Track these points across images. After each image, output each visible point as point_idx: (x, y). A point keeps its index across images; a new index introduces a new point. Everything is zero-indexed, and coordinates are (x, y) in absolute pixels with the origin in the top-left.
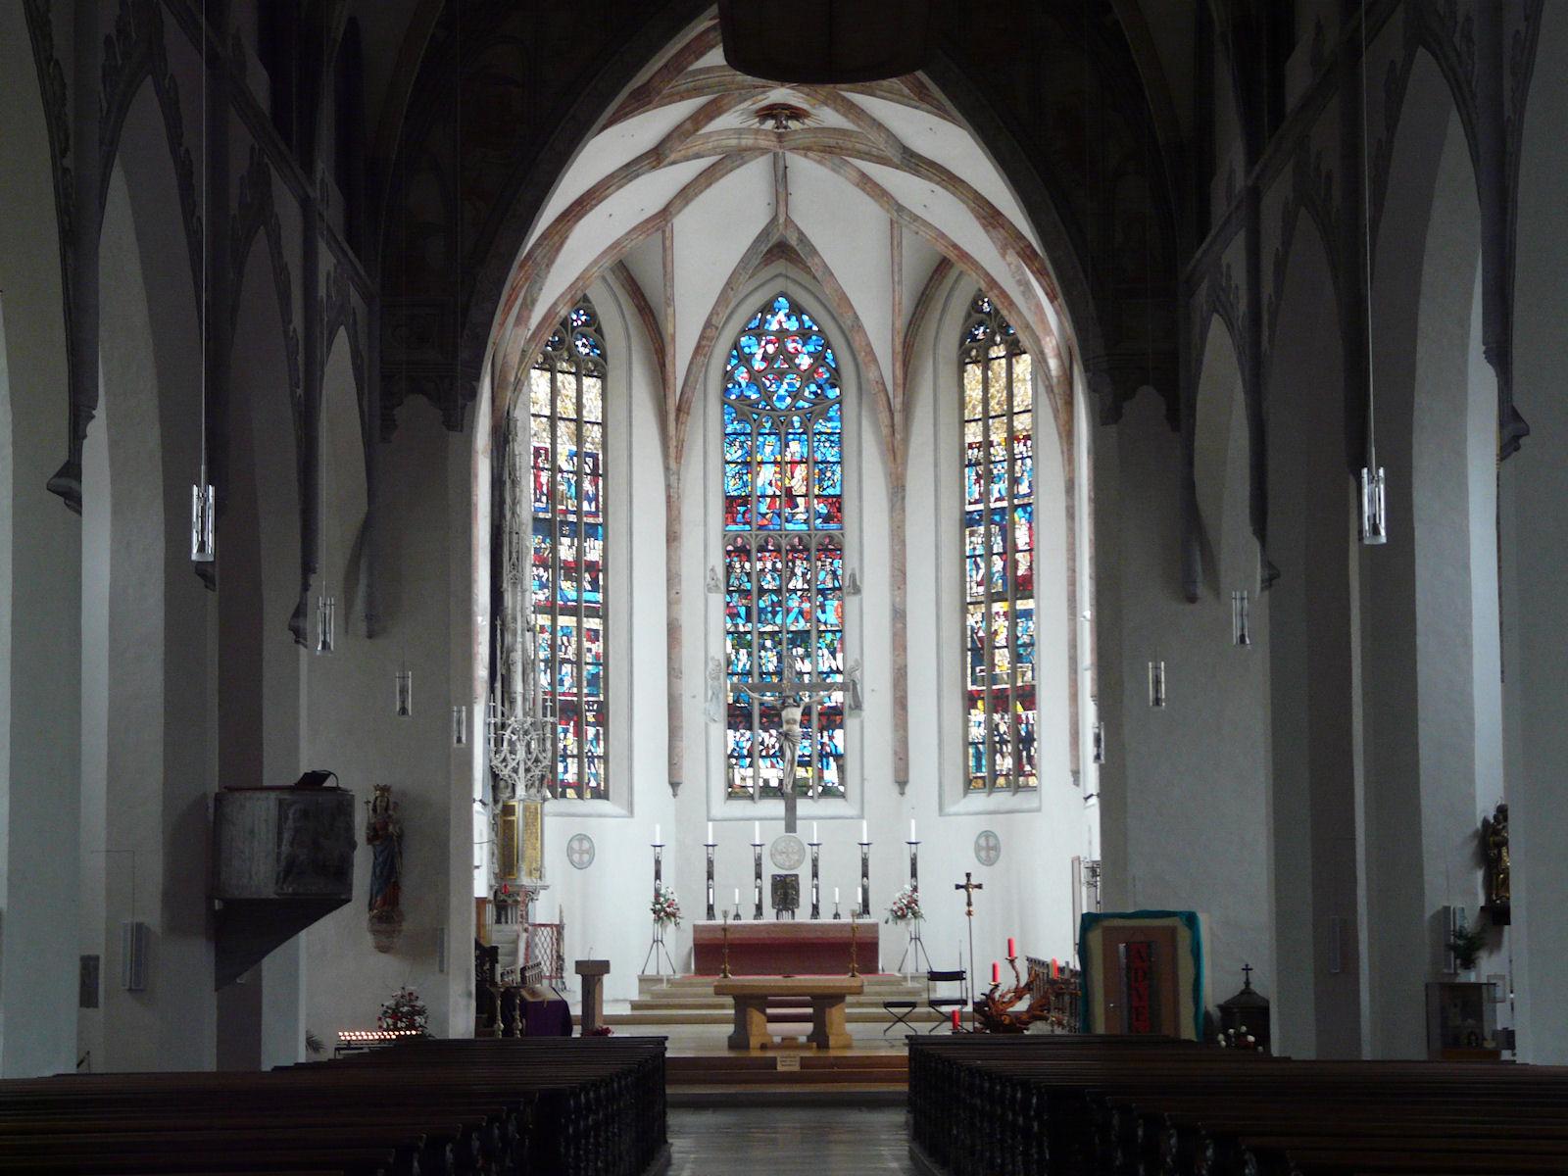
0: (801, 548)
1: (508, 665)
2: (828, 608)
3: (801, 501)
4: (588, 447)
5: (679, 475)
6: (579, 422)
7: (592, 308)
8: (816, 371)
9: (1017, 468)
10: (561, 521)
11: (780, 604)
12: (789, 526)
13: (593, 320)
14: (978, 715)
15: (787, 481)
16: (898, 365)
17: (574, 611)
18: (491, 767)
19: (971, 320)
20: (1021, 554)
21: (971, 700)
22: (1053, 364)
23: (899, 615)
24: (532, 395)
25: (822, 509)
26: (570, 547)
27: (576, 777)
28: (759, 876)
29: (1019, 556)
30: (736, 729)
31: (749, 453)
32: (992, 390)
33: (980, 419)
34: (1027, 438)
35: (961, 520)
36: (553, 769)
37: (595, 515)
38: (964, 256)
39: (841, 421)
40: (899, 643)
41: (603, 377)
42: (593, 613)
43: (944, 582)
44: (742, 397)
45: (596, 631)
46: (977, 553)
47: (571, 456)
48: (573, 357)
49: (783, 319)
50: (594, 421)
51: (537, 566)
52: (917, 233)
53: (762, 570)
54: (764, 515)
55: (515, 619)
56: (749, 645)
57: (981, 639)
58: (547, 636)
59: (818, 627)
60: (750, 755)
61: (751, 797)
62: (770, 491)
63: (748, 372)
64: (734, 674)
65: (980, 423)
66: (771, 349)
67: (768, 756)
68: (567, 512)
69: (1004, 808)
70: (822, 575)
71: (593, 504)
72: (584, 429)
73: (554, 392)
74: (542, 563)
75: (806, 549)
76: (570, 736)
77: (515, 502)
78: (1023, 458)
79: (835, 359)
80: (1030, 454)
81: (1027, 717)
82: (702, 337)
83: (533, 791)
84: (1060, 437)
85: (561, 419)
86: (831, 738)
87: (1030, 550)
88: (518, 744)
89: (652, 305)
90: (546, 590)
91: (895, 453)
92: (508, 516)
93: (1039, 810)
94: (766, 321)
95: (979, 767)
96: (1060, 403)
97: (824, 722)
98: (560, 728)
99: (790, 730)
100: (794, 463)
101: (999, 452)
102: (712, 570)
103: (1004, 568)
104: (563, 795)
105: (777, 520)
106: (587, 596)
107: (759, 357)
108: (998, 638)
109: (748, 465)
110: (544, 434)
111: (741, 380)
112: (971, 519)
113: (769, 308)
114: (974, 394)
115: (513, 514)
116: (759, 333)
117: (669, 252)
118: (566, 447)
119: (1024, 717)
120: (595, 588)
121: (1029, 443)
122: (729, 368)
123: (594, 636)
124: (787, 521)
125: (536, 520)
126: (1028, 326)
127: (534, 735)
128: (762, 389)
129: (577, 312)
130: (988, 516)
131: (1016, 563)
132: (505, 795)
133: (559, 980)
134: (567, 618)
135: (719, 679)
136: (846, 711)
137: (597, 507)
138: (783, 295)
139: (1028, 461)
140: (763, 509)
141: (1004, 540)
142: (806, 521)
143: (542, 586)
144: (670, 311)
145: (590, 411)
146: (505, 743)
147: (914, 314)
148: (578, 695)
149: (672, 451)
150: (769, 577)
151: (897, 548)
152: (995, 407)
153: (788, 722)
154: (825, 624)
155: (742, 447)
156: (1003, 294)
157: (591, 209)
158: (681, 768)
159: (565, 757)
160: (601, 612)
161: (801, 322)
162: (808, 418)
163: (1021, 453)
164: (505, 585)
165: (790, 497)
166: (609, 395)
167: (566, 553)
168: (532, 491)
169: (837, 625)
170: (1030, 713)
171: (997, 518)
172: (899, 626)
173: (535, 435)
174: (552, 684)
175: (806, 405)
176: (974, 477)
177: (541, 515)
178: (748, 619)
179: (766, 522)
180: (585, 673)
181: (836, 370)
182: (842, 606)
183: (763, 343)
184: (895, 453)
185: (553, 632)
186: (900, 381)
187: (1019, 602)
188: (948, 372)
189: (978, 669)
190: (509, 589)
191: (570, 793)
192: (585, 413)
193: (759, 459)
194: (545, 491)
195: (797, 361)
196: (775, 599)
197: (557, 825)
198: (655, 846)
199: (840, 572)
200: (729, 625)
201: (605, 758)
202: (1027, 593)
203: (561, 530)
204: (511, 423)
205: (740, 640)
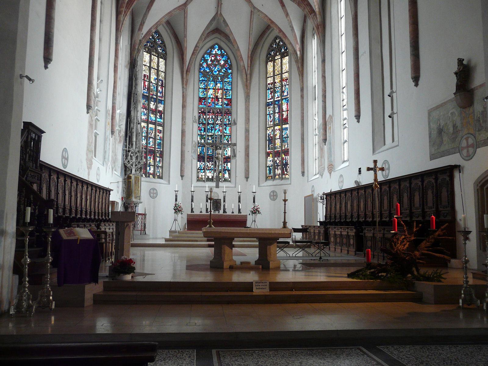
0: (220, 112)
1: (131, 133)
2: (227, 129)
3: (220, 100)
4: (160, 78)
5: (186, 89)
6: (158, 70)
7: (163, 39)
8: (225, 65)
9: (284, 88)
10: (151, 97)
11: (213, 127)
12: (217, 106)
13: (163, 42)
15: (216, 94)
16: (249, 62)
17: (154, 123)
19: (270, 50)
20: (284, 112)
22: (298, 53)
23: (247, 131)
24: (144, 59)
25: (226, 102)
26: (154, 105)
27: (153, 172)
29: (284, 113)
30: (200, 162)
31: (206, 86)
32: (276, 68)
33: (272, 76)
34: (287, 79)
35: (266, 104)
37: (162, 97)
38: (272, 22)
39: (232, 78)
40: (247, 138)
41: (165, 59)
42: (160, 125)
44: (204, 70)
46: (271, 113)
47: (155, 79)
48: (157, 52)
49: (217, 51)
50: (162, 71)
51: (143, 109)
52: (259, 15)
53: (209, 118)
54: (210, 103)
55: (134, 120)
56: (205, 138)
57: (271, 137)
58: (145, 129)
59: (224, 134)
60: (204, 169)
61: (204, 181)
62: (211, 97)
63: (207, 64)
64: (200, 146)
65: (272, 77)
66: (213, 58)
67: (209, 170)
68: (153, 95)
70: (226, 120)
71: (161, 94)
72: (159, 73)
73: (151, 60)
74: (144, 107)
75: (221, 113)
77: (136, 84)
78: (285, 85)
79: (230, 62)
80: (287, 84)
81: (286, 158)
82: (194, 50)
83: (138, 172)
85: (152, 68)
86: (227, 165)
87: (287, 111)
88: (133, 157)
89: (180, 41)
90: (146, 116)
91: (247, 87)
92: (134, 88)
93: (290, 184)
94: (212, 51)
95: (270, 173)
96: (300, 65)
97: (225, 160)
98: (148, 157)
99: (218, 156)
100: (218, 89)
101: (278, 85)
102: (195, 117)
103: (279, 116)
104: (149, 177)
105: (213, 104)
106: (158, 120)
107: (209, 60)
109: (206, 89)
110: (147, 71)
111: (205, 66)
112: (269, 104)
113: (213, 47)
114: (270, 70)
115: (135, 88)
116: (210, 54)
118: (153, 77)
119: (285, 158)
120: (161, 118)
121: (287, 81)
122: (201, 63)
123: (160, 132)
124: (216, 105)
125: (143, 95)
126: (291, 43)
127: (138, 154)
128: (210, 69)
130: (274, 103)
131: (283, 115)
132: (128, 173)
133: (144, 231)
134: (152, 125)
135: (196, 147)
136: (231, 158)
137: (162, 95)
139: (287, 86)
140: (210, 101)
141: (279, 109)
142: (221, 105)
143: (145, 115)
145: (161, 68)
146: (129, 156)
147: (254, 48)
148: (155, 148)
149: (185, 83)
150: (211, 120)
153: (217, 154)
154: (226, 133)
155: (204, 84)
156: (284, 33)
158: (184, 171)
159: (150, 165)
160: (162, 125)
161: (222, 52)
163: (285, 84)
164: (131, 109)
165: (217, 98)
166: (167, 64)
167: (152, 106)
168: (143, 87)
169: (229, 134)
170: (287, 157)
171: (277, 103)
172: (247, 134)
173: (144, 71)
174: (147, 143)
175: (222, 74)
177: (145, 94)
178: (204, 131)
179: (210, 105)
180: (157, 142)
181: (231, 65)
182: (231, 129)
183: (211, 57)
184: (247, 87)
185: (147, 128)
186: (250, 66)
189: (270, 145)
190: (133, 110)
191: (151, 176)
192: (160, 68)
193: (209, 88)
194: (147, 87)
195: (220, 62)
196: (212, 126)
197: (145, 185)
198: (176, 191)
199: (230, 119)
200: (199, 133)
201: (162, 167)
202: (286, 123)
204: (136, 61)
205: (202, 137)
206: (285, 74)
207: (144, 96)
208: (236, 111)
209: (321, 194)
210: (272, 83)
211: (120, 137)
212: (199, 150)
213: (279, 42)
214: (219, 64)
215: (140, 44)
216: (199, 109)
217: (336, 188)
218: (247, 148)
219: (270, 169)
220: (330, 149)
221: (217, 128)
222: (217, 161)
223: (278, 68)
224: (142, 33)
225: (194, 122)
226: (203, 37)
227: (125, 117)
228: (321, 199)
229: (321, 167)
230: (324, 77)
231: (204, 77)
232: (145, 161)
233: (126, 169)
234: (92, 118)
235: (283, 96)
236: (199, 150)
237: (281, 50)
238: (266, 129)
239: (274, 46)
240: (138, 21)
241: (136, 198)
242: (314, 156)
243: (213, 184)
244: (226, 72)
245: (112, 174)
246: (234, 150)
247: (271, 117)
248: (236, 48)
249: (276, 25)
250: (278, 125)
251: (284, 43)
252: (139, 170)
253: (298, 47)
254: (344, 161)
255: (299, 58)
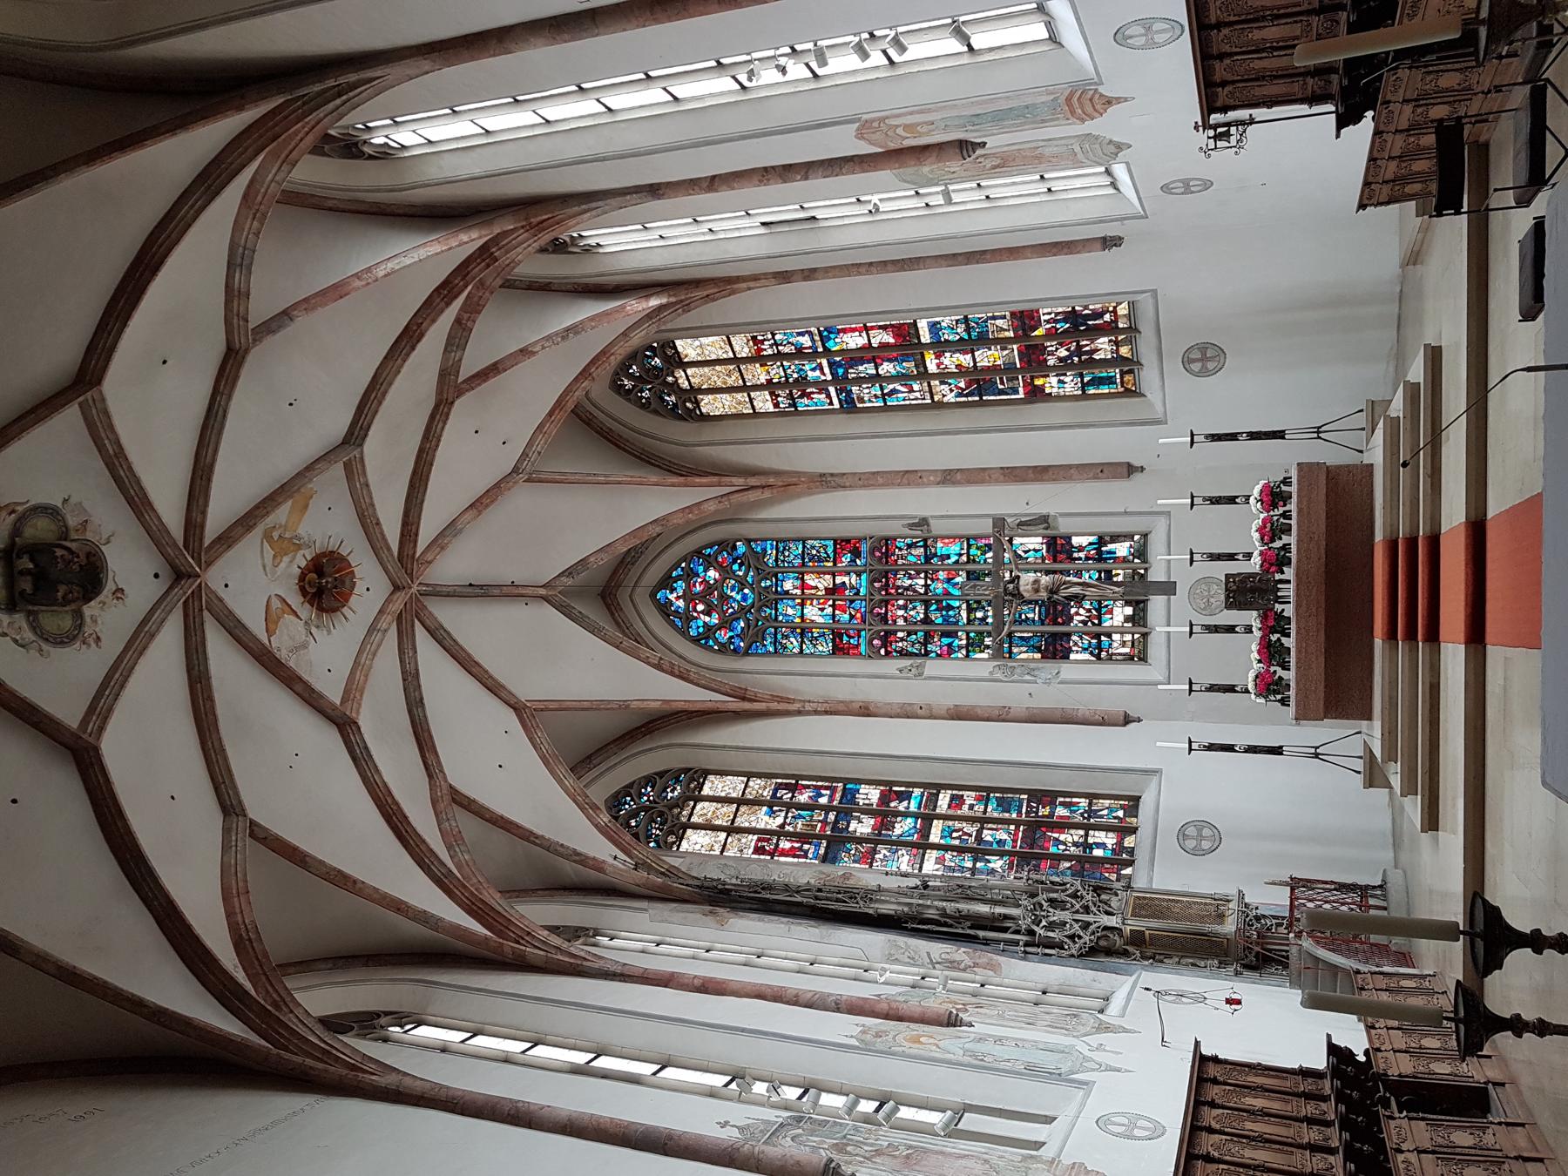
1: (960, 917)
2: (945, 551)
3: (839, 580)
4: (767, 794)
6: (741, 802)
9: (786, 350)
11: (939, 602)
12: (863, 591)
13: (649, 780)
14: (1051, 384)
16: (704, 480)
17: (927, 819)
18: (1081, 955)
21: (1036, 394)
22: (654, 302)
23: (949, 477)
27: (1111, 835)
28: (1231, 629)
30: (1070, 650)
31: (793, 630)
32: (719, 384)
34: (754, 338)
36: (1101, 861)
37: (833, 790)
38: (559, 404)
41: (706, 773)
43: (911, 428)
45: (953, 798)
47: (772, 813)
53: (906, 619)
54: (852, 617)
58: (948, 856)
60: (1097, 636)
61: (1145, 635)
62: (829, 610)
64: (1010, 652)
66: (700, 607)
67: (1099, 617)
68: (824, 822)
69: (1154, 340)
70: (911, 558)
73: (709, 827)
74: (869, 858)
76: (1062, 837)
77: (787, 888)
78: (776, 344)
81: (1048, 322)
82: (672, 674)
83: (1114, 903)
84: (733, 292)
86: (1081, 549)
87: (867, 329)
91: (789, 484)
92: (798, 899)
93: (1154, 292)
97: (1063, 556)
98: (1053, 850)
101: (776, 373)
103: (890, 360)
104: (1131, 851)
105: (857, 604)
107: (707, 619)
108: (965, 364)
109: (804, 630)
113: (665, 609)
116: (688, 618)
117: (564, 705)
118: (763, 819)
123: (956, 801)
125: (824, 859)
126: (624, 334)
127: (1042, 898)
129: (641, 795)
131: (883, 346)
137: (826, 788)
138: (653, 595)
140: (846, 617)
141: (862, 361)
142: (859, 575)
144: (634, 705)
146: (1051, 934)
148: (1017, 823)
149: (781, 708)
151: (881, 481)
152: (734, 380)
153: (1037, 591)
155: (787, 637)
157: (397, 804)
159: (1087, 846)
160: (934, 789)
161: (679, 578)
162: (763, 573)
165: (834, 591)
167: (863, 826)
171: (841, 371)
174: (1001, 854)
176: (805, 401)
177: (822, 851)
178: (953, 634)
180: (996, 815)
182: (943, 538)
184: (789, 484)
185: (946, 848)
186: (715, 479)
187: (923, 340)
188: (708, 432)
192: (734, 795)
197: (1165, 872)
199: (908, 541)
201: (1092, 797)
203: (842, 830)
205: (973, 645)
206: (737, 348)
207: (829, 858)
208: (872, 522)
209: (1203, 138)
210: (772, 394)
211: (976, 965)
212: (1023, 656)
213: (631, 377)
214: (719, 583)
215: (649, 869)
216: (873, 654)
217: (1177, 63)
218: (1013, 475)
219: (1092, 383)
220: (1001, 118)
221: (939, 591)
222: (1064, 593)
223: (717, 376)
224: (611, 861)
225: (921, 674)
226: (627, 643)
227: (902, 940)
228: (1227, 135)
229: (1080, 156)
230: (713, 183)
231: (764, 639)
232: (1067, 864)
233: (1104, 950)
234: (879, 1153)
235: (813, 347)
236: (1023, 656)
237: (655, 367)
238: (940, 405)
239: (646, 394)
240: (570, 869)
241: (1221, 917)
242: (1037, 199)
243: (1156, 604)
244: (743, 561)
245: (1126, 1031)
246: (1020, 524)
247: (894, 391)
248: (658, 529)
249: (568, 391)
250: (922, 363)
251: (633, 357)
252: (1103, 897)
253: (638, 306)
254: (1053, 39)
255: (673, 299)
